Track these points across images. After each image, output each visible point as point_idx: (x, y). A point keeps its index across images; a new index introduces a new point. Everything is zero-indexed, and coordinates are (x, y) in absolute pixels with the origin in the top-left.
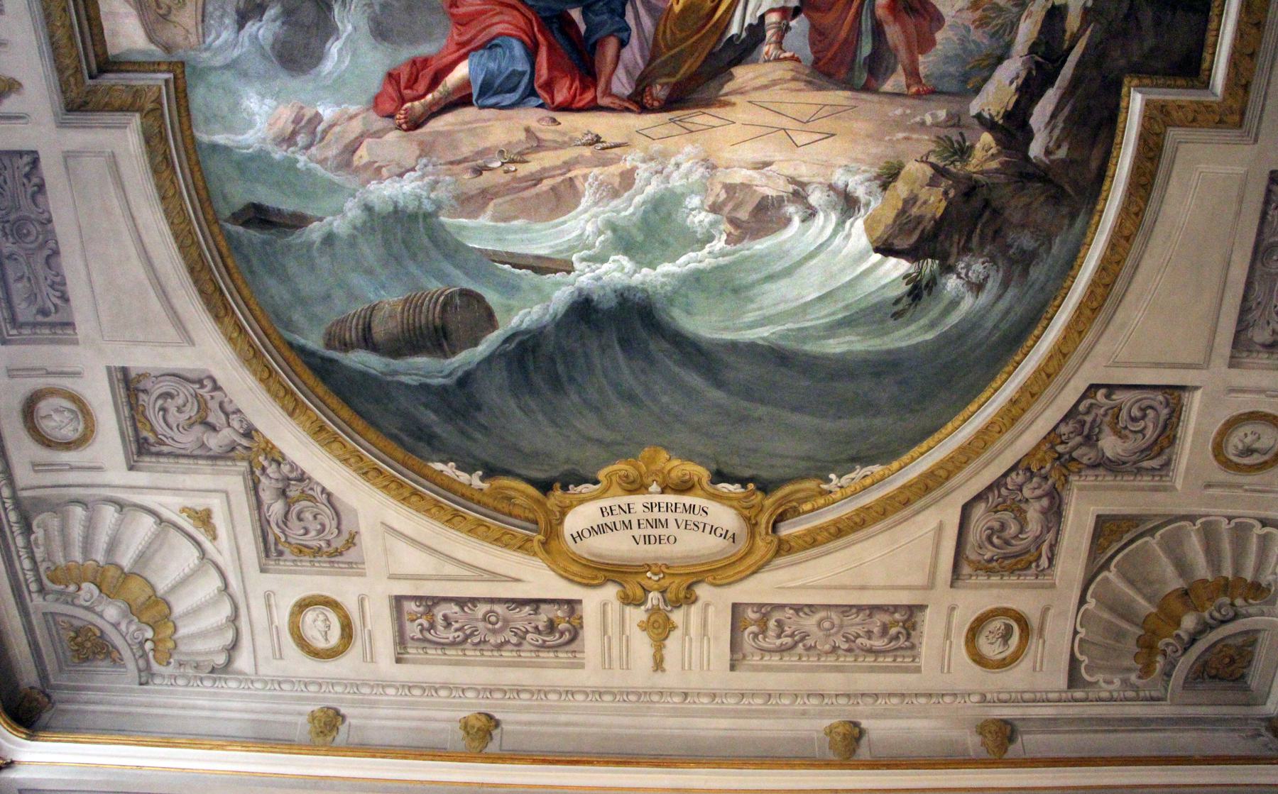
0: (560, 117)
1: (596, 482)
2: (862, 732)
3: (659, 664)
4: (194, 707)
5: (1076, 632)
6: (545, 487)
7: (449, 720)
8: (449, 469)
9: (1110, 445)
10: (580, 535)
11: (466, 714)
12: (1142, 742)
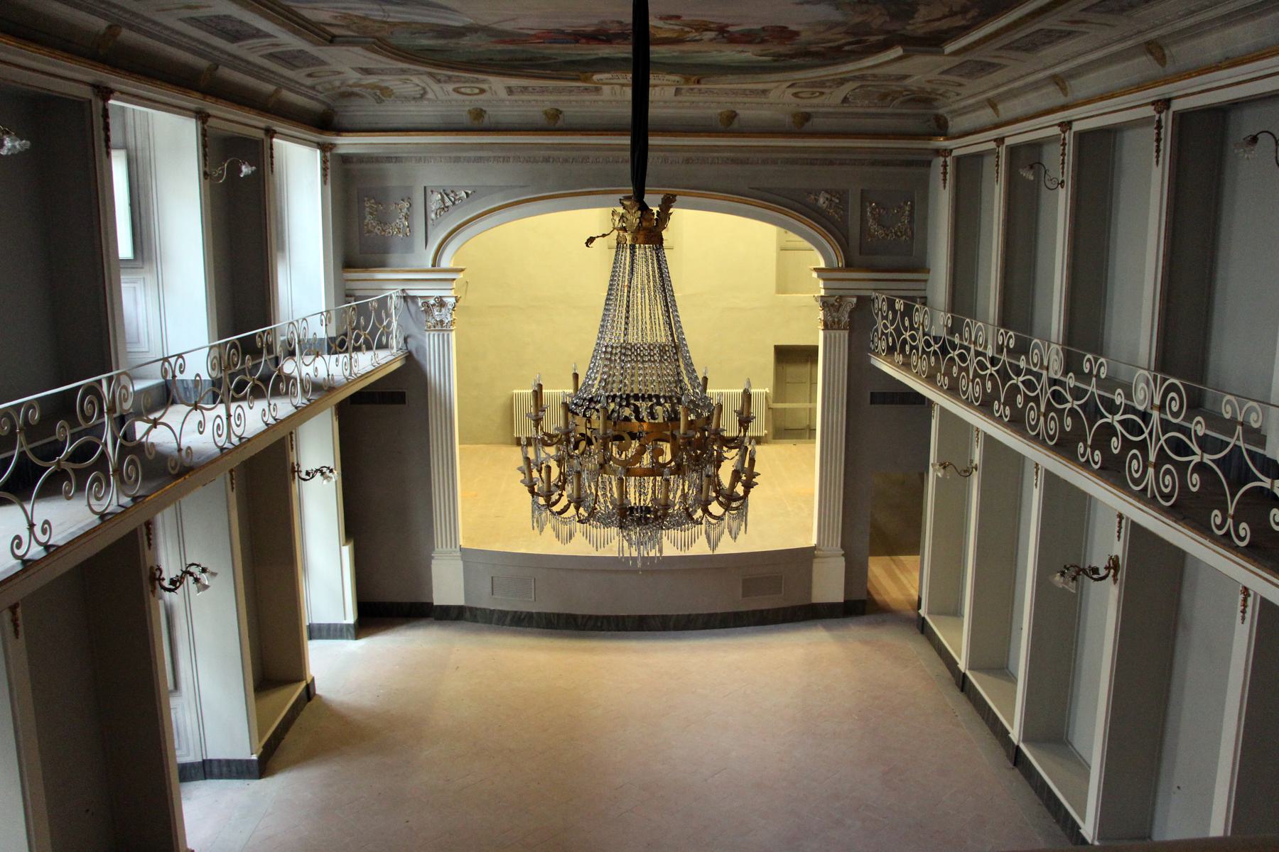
4: (410, 111)
11: (545, 109)
12: (869, 124)
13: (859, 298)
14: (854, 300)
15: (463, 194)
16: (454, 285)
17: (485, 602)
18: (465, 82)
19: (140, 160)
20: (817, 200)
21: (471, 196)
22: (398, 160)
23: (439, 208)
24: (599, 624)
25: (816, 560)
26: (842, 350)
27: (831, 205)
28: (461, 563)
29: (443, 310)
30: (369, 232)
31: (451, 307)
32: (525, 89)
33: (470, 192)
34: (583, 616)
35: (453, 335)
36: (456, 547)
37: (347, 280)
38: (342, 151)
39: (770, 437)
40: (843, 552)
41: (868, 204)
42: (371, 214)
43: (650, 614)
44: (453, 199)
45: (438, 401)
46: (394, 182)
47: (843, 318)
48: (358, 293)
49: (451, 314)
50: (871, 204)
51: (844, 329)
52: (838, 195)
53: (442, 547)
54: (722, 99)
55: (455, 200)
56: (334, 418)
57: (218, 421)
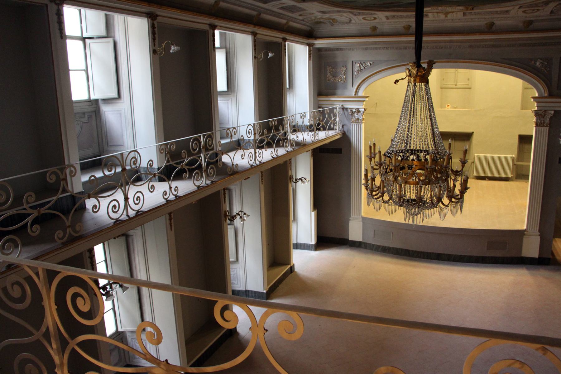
2: (494, 24)
13: (555, 111)
14: (553, 112)
15: (369, 64)
16: (364, 103)
18: (366, 15)
19: (231, 52)
20: (535, 63)
21: (372, 65)
22: (341, 49)
23: (358, 70)
25: (524, 236)
27: (543, 66)
28: (361, 223)
29: (359, 114)
30: (328, 80)
31: (362, 113)
32: (394, 17)
33: (371, 63)
34: (412, 251)
35: (363, 125)
36: (360, 216)
37: (319, 101)
38: (317, 46)
39: (514, 178)
40: (539, 234)
42: (330, 73)
43: (443, 253)
44: (364, 66)
45: (355, 154)
46: (339, 59)
47: (546, 121)
48: (323, 106)
49: (362, 116)
54: (487, 16)
55: (365, 66)
56: (311, 158)
57: (251, 154)
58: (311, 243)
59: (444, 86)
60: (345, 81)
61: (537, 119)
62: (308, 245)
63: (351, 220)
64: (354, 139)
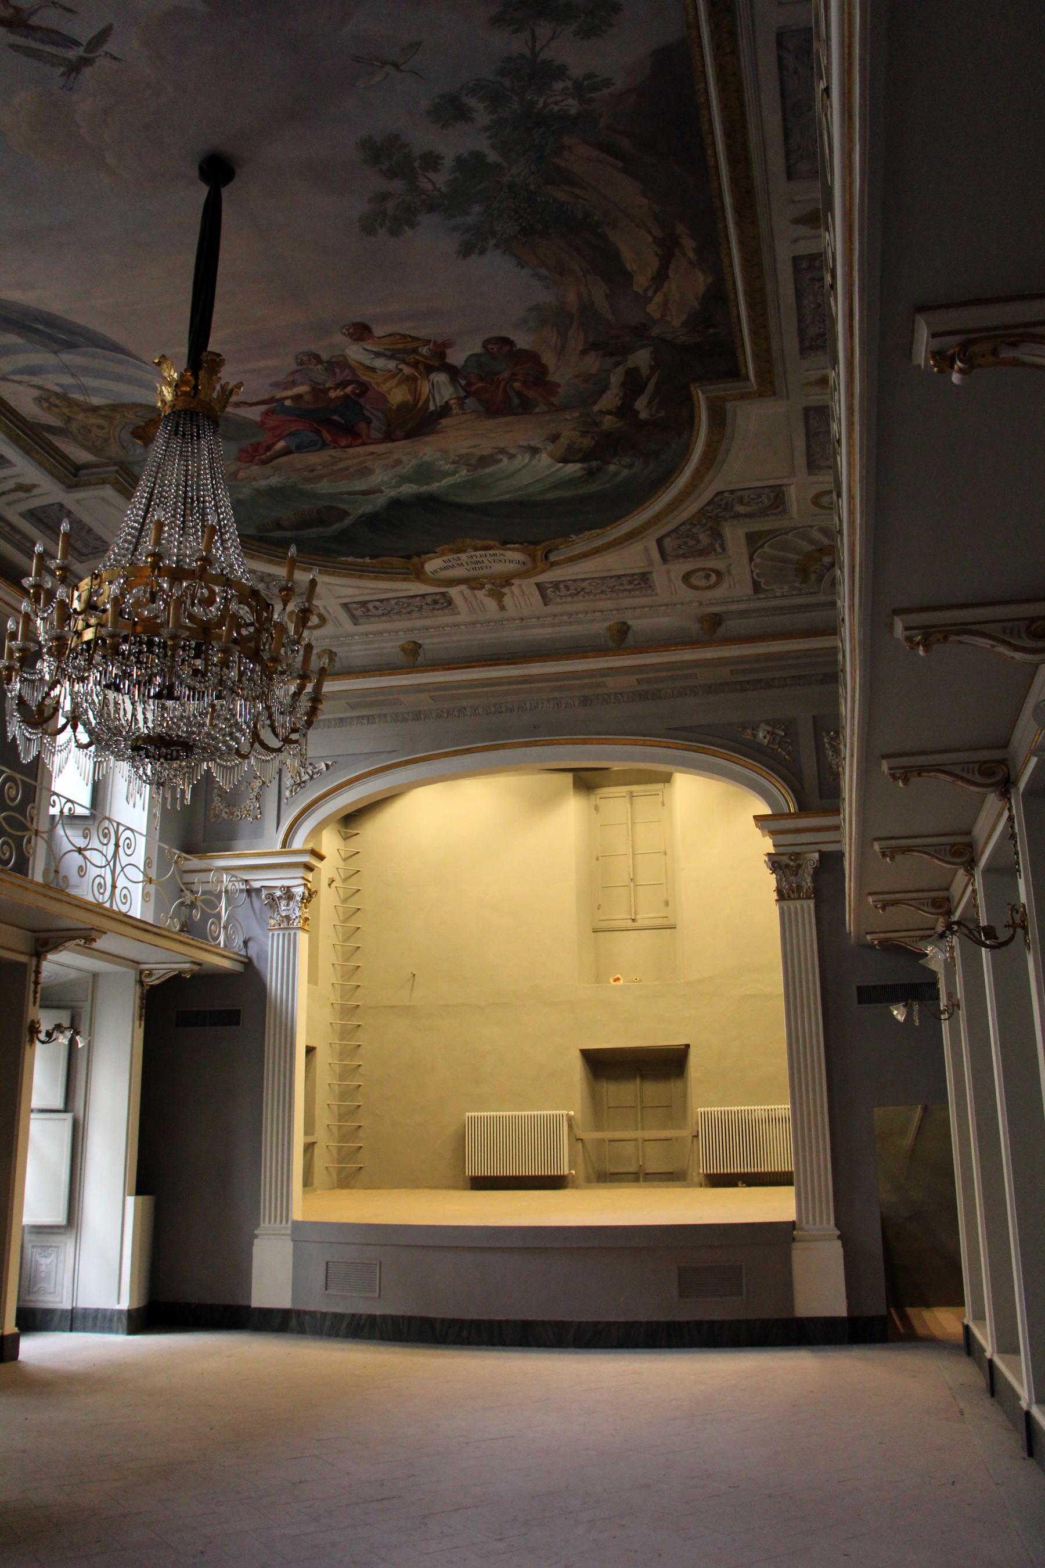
0: (347, 450)
1: (435, 553)
2: (629, 628)
3: (502, 608)
5: (752, 572)
6: (409, 557)
7: (393, 647)
8: (351, 559)
9: (740, 509)
10: (436, 571)
11: (401, 643)
14: (816, 855)
15: (323, 766)
17: (317, 1303)
20: (755, 736)
21: (331, 768)
24: (465, 1333)
25: (795, 1245)
26: (807, 926)
27: (774, 739)
28: (291, 1243)
29: (291, 903)
30: (216, 816)
31: (299, 899)
33: (330, 763)
34: (443, 1320)
36: (287, 1221)
37: (185, 872)
40: (838, 1233)
41: (824, 734)
42: (219, 795)
43: (540, 1319)
44: (310, 772)
45: (278, 1021)
47: (804, 883)
50: (828, 734)
51: (808, 898)
52: (783, 727)
53: (270, 1222)
55: (313, 773)
56: (137, 1023)
58: (118, 1307)
59: (603, 925)
60: (259, 816)
61: (781, 880)
62: (108, 1313)
63: (260, 1237)
64: (274, 982)
